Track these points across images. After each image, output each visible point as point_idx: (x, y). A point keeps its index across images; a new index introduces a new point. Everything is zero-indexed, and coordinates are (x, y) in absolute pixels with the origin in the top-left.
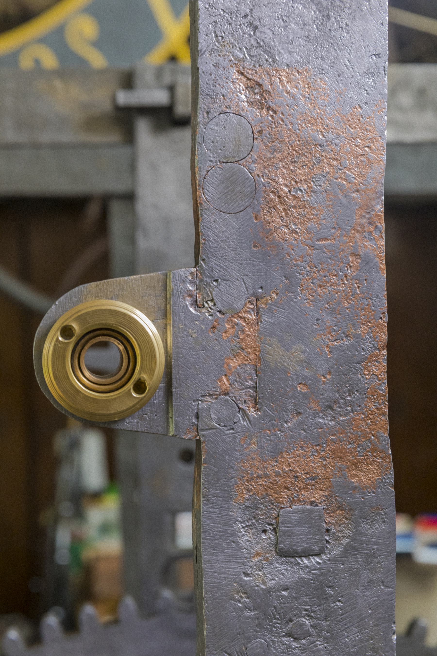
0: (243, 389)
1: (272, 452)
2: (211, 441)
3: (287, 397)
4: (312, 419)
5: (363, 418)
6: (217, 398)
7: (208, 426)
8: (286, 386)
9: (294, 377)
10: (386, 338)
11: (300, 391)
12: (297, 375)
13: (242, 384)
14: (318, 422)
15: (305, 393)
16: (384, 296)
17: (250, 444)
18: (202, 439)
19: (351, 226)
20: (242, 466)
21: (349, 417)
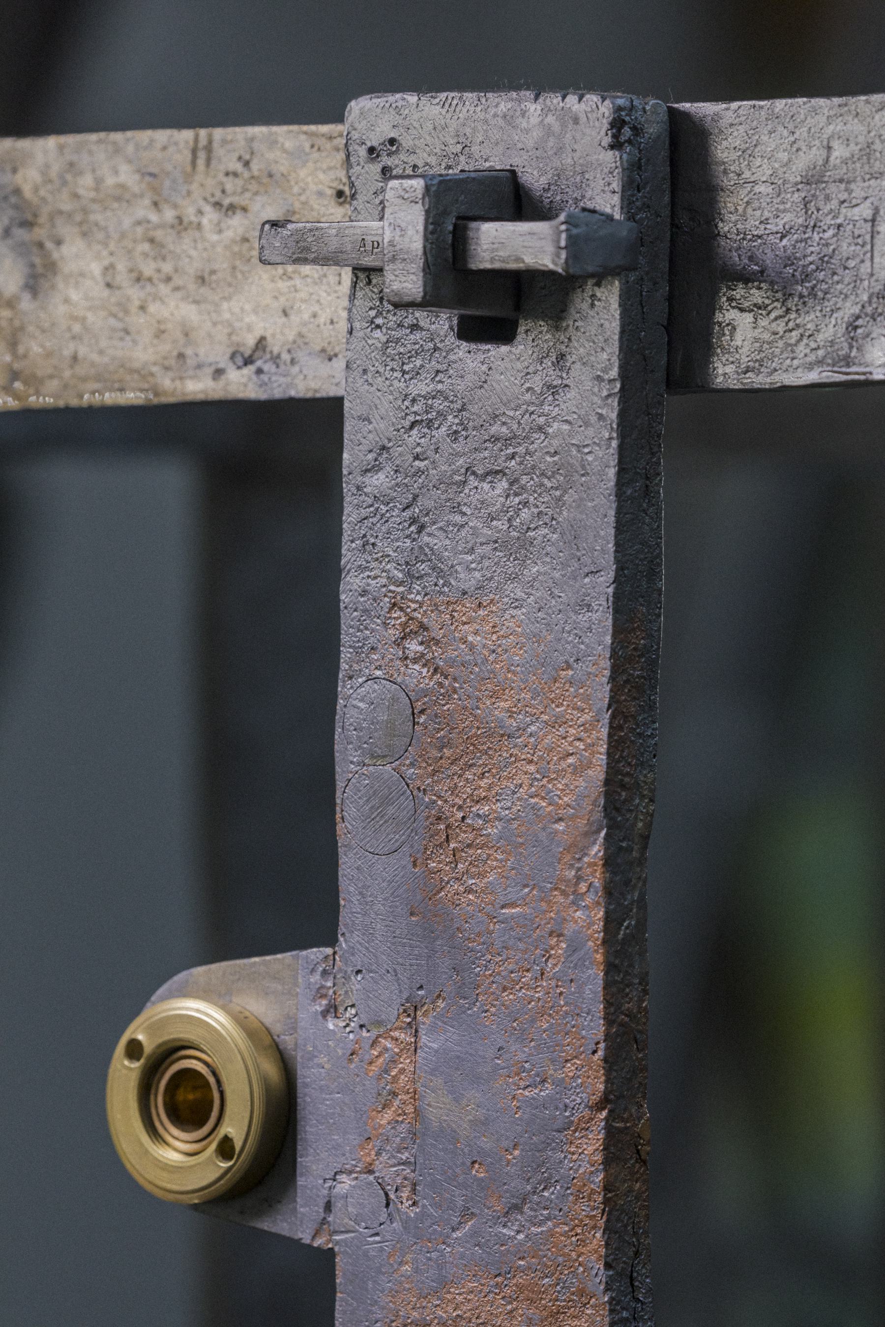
0: (394, 1166)
1: (432, 1281)
2: (347, 1253)
3: (455, 1183)
4: (490, 1227)
5: (566, 1232)
6: (356, 1178)
7: (344, 1227)
8: (455, 1164)
9: (466, 1150)
10: (602, 1087)
11: (475, 1176)
12: (470, 1145)
13: (394, 1157)
14: (500, 1232)
15: (482, 1180)
16: (600, 1012)
17: (401, 1263)
18: (336, 1249)
19: (551, 883)
20: (391, 1301)
21: (544, 1229)
